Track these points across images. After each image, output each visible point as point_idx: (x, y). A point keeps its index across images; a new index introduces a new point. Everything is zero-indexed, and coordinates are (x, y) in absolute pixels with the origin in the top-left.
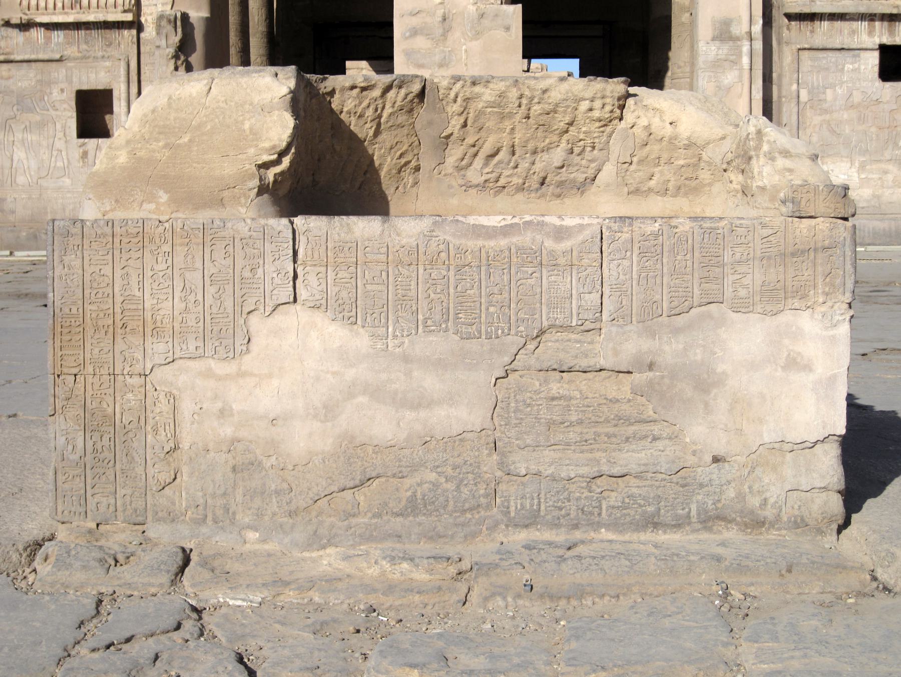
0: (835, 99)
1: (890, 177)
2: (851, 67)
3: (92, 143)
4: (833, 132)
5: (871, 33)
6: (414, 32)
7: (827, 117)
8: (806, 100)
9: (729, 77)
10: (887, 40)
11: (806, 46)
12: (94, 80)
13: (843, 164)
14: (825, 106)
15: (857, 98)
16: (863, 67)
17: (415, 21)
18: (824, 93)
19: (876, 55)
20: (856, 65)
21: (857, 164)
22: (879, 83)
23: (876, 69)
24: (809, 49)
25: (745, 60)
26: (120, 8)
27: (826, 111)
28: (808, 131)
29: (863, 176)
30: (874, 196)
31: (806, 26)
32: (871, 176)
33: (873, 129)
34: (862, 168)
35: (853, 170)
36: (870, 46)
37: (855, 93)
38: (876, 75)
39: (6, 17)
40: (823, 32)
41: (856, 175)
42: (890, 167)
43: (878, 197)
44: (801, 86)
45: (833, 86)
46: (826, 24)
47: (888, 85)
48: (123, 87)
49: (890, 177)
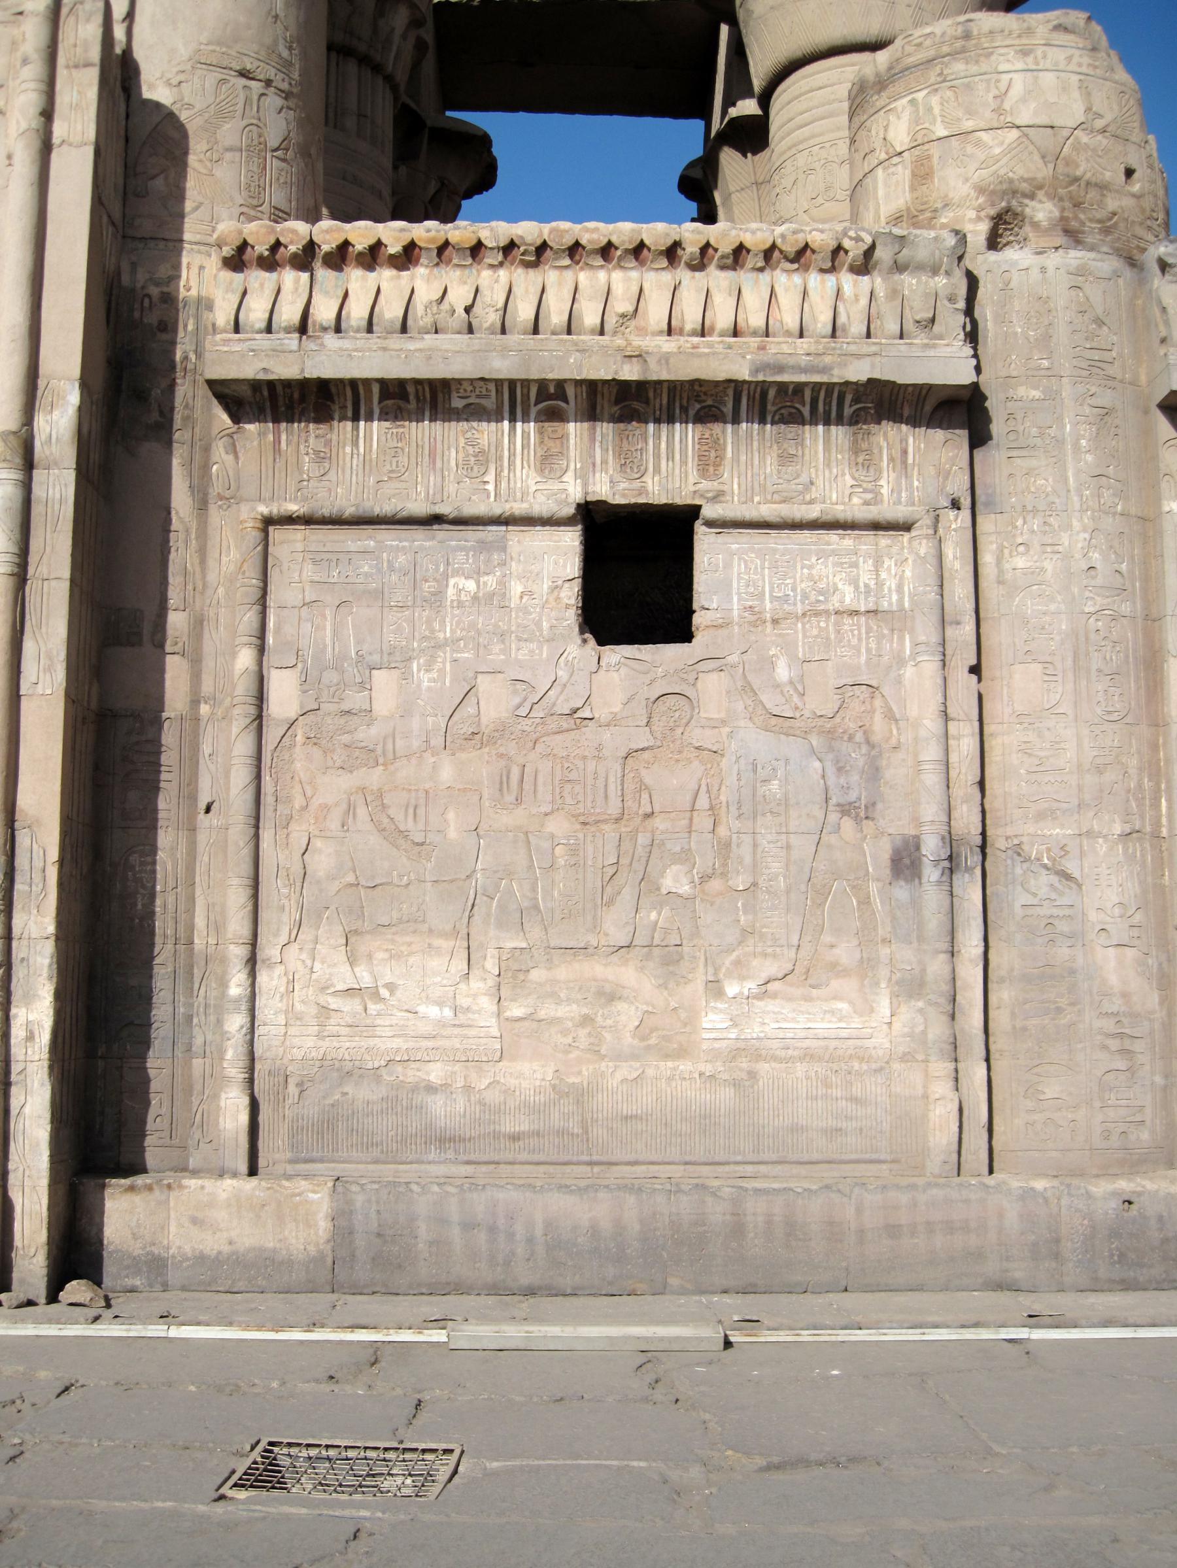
0: (406, 711)
1: (627, 1015)
2: (471, 585)
4: (395, 835)
5: (547, 463)
7: (374, 778)
8: (292, 712)
10: (610, 487)
11: (293, 508)
13: (435, 963)
14: (367, 734)
15: (494, 703)
16: (516, 588)
18: (365, 685)
19: (571, 540)
20: (491, 581)
21: (491, 965)
23: (571, 594)
24: (308, 520)
27: (371, 756)
28: (298, 834)
29: (516, 1010)
30: (560, 1091)
31: (302, 439)
32: (548, 1010)
33: (558, 826)
34: (511, 977)
35: (476, 984)
36: (541, 506)
37: (484, 684)
38: (571, 617)
40: (363, 461)
41: (487, 1004)
42: (626, 974)
43: (580, 1095)
44: (270, 659)
45: (397, 660)
46: (375, 431)
47: (616, 654)
49: (627, 1015)
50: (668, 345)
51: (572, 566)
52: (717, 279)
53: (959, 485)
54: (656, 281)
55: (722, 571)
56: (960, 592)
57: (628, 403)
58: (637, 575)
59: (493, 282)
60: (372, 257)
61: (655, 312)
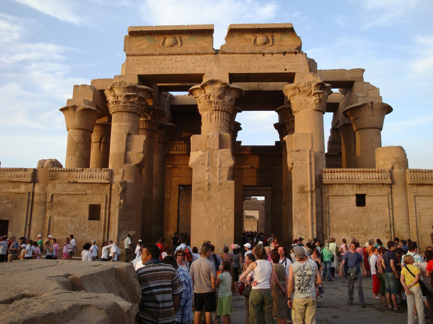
3: (93, 222)
5: (353, 190)
6: (199, 189)
9: (304, 205)
10: (359, 193)
12: (95, 202)
17: (199, 185)
19: (355, 197)
22: (356, 207)
23: (355, 202)
25: (309, 200)
26: (105, 178)
39: (69, 180)
41: (349, 238)
48: (104, 204)
50: (364, 180)
51: (355, 200)
52: (368, 174)
53: (390, 192)
54: (362, 174)
55: (368, 200)
56: (390, 201)
57: (360, 185)
58: (361, 200)
59: (347, 174)
60: (337, 172)
61: (362, 178)
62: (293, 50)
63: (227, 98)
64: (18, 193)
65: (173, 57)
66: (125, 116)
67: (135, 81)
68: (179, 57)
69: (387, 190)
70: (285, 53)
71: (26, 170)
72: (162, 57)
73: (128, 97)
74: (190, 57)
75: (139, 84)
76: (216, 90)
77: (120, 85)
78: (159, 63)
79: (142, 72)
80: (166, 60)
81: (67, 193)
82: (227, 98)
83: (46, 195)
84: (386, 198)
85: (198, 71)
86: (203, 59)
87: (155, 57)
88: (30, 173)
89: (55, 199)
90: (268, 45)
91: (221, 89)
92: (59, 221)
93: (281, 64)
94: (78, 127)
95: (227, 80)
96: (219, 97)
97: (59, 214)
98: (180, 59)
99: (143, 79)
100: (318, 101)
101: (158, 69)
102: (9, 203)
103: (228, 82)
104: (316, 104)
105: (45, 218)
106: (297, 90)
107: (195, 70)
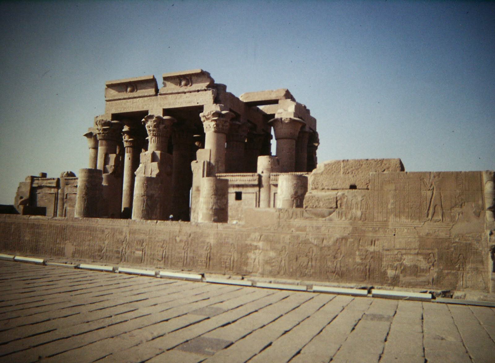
55: (243, 196)
57: (238, 186)
62: (203, 88)
63: (162, 126)
64: (50, 193)
65: (131, 100)
66: (104, 142)
67: (109, 119)
68: (135, 99)
69: (257, 189)
70: (198, 91)
71: (54, 179)
72: (125, 101)
73: (104, 130)
74: (141, 99)
75: (112, 120)
76: (152, 122)
77: (100, 122)
78: (123, 104)
79: (114, 111)
80: (127, 102)
81: (73, 193)
82: (162, 126)
83: (63, 194)
84: (255, 194)
85: (145, 109)
86: (149, 99)
87: (121, 101)
88: (55, 181)
89: (68, 197)
90: (188, 85)
91: (154, 121)
92: (70, 210)
93: (195, 99)
94: (94, 147)
95: (161, 115)
96: (155, 126)
97: (70, 206)
98: (135, 101)
99: (114, 116)
100: (215, 126)
101: (122, 109)
102: (46, 199)
103: (162, 116)
104: (214, 128)
105: (63, 208)
106: (205, 118)
107: (143, 108)
